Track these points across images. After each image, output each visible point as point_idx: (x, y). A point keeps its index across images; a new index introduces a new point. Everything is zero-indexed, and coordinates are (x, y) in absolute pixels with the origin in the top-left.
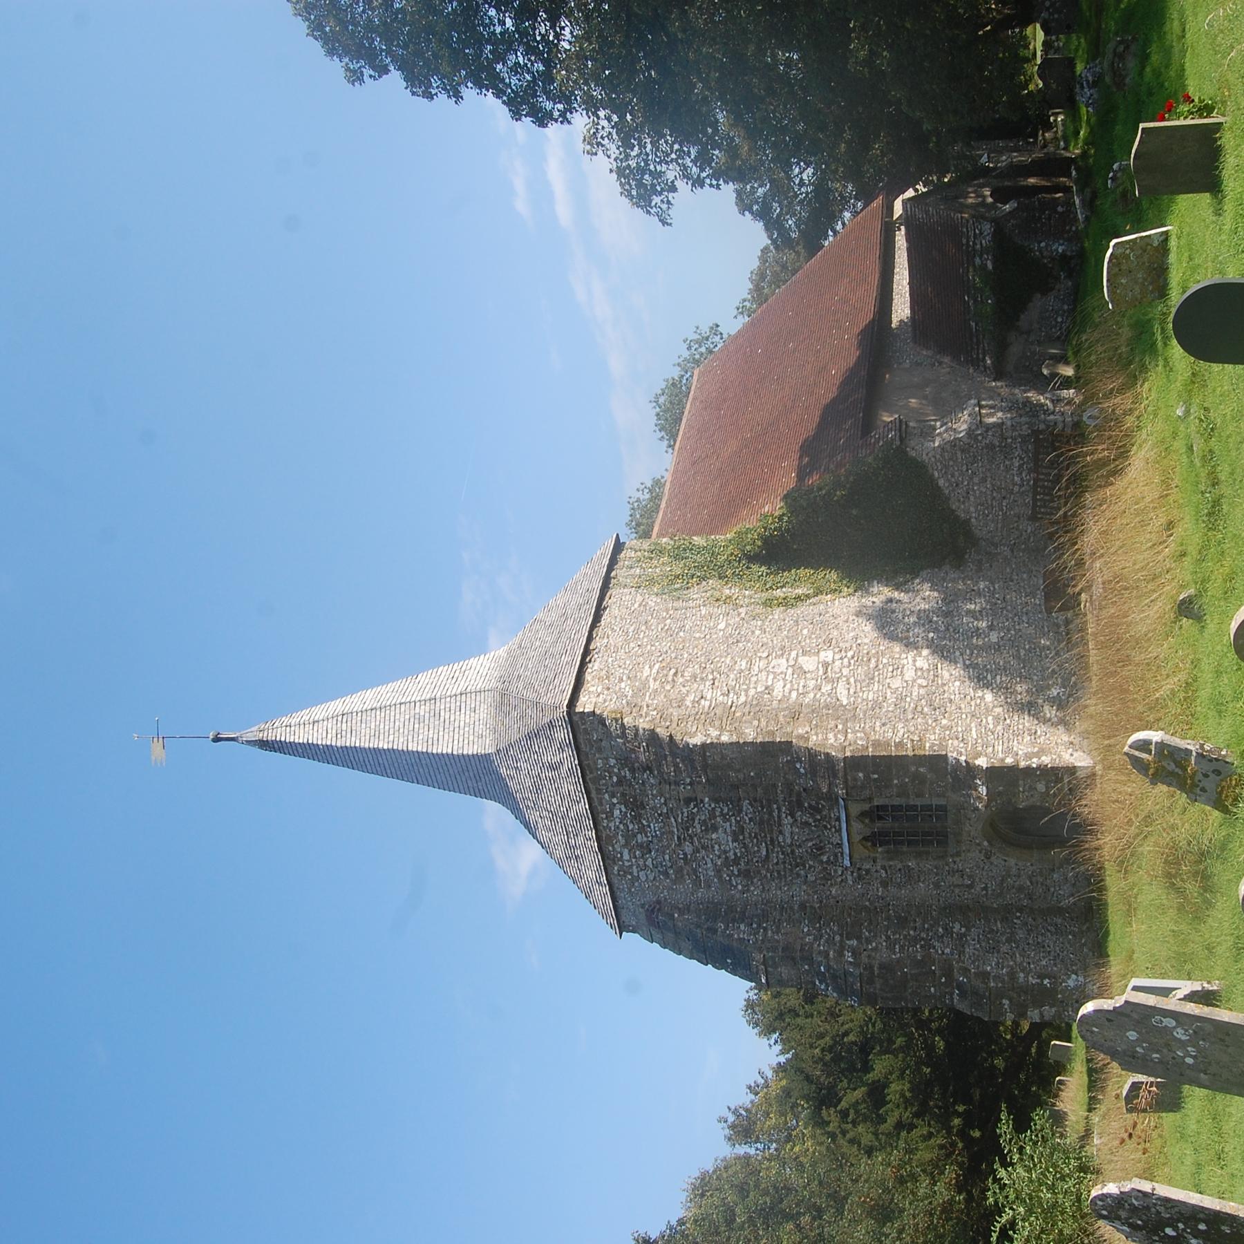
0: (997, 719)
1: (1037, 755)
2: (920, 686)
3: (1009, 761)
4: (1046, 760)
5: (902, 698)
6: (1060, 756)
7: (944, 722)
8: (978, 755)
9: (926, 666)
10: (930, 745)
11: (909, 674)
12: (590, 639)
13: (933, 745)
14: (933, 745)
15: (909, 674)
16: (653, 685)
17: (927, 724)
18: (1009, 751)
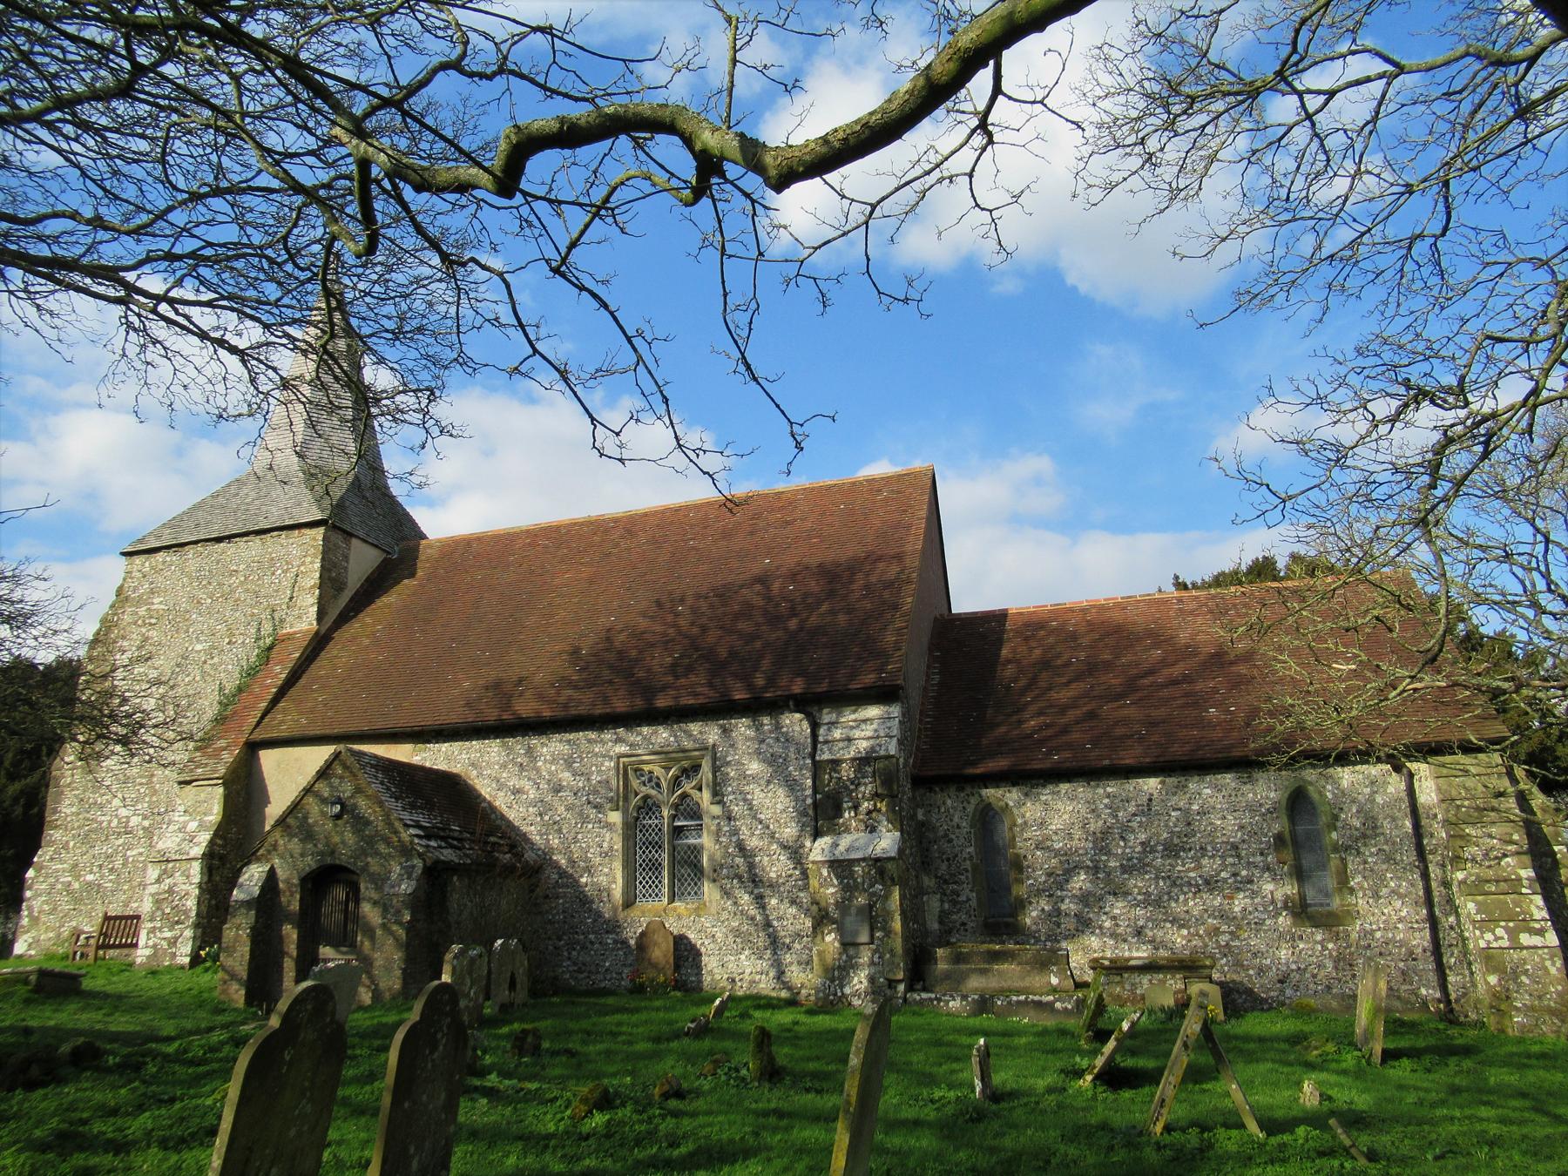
0: (70, 884)
1: (30, 915)
2: (110, 822)
3: (28, 894)
4: (25, 921)
5: (101, 807)
6: (28, 932)
7: (72, 844)
8: (38, 870)
9: (131, 824)
10: (53, 835)
11: (123, 812)
12: (196, 542)
13: (51, 836)
14: (51, 836)
15: (123, 812)
16: (142, 611)
17: (73, 829)
18: (37, 895)
